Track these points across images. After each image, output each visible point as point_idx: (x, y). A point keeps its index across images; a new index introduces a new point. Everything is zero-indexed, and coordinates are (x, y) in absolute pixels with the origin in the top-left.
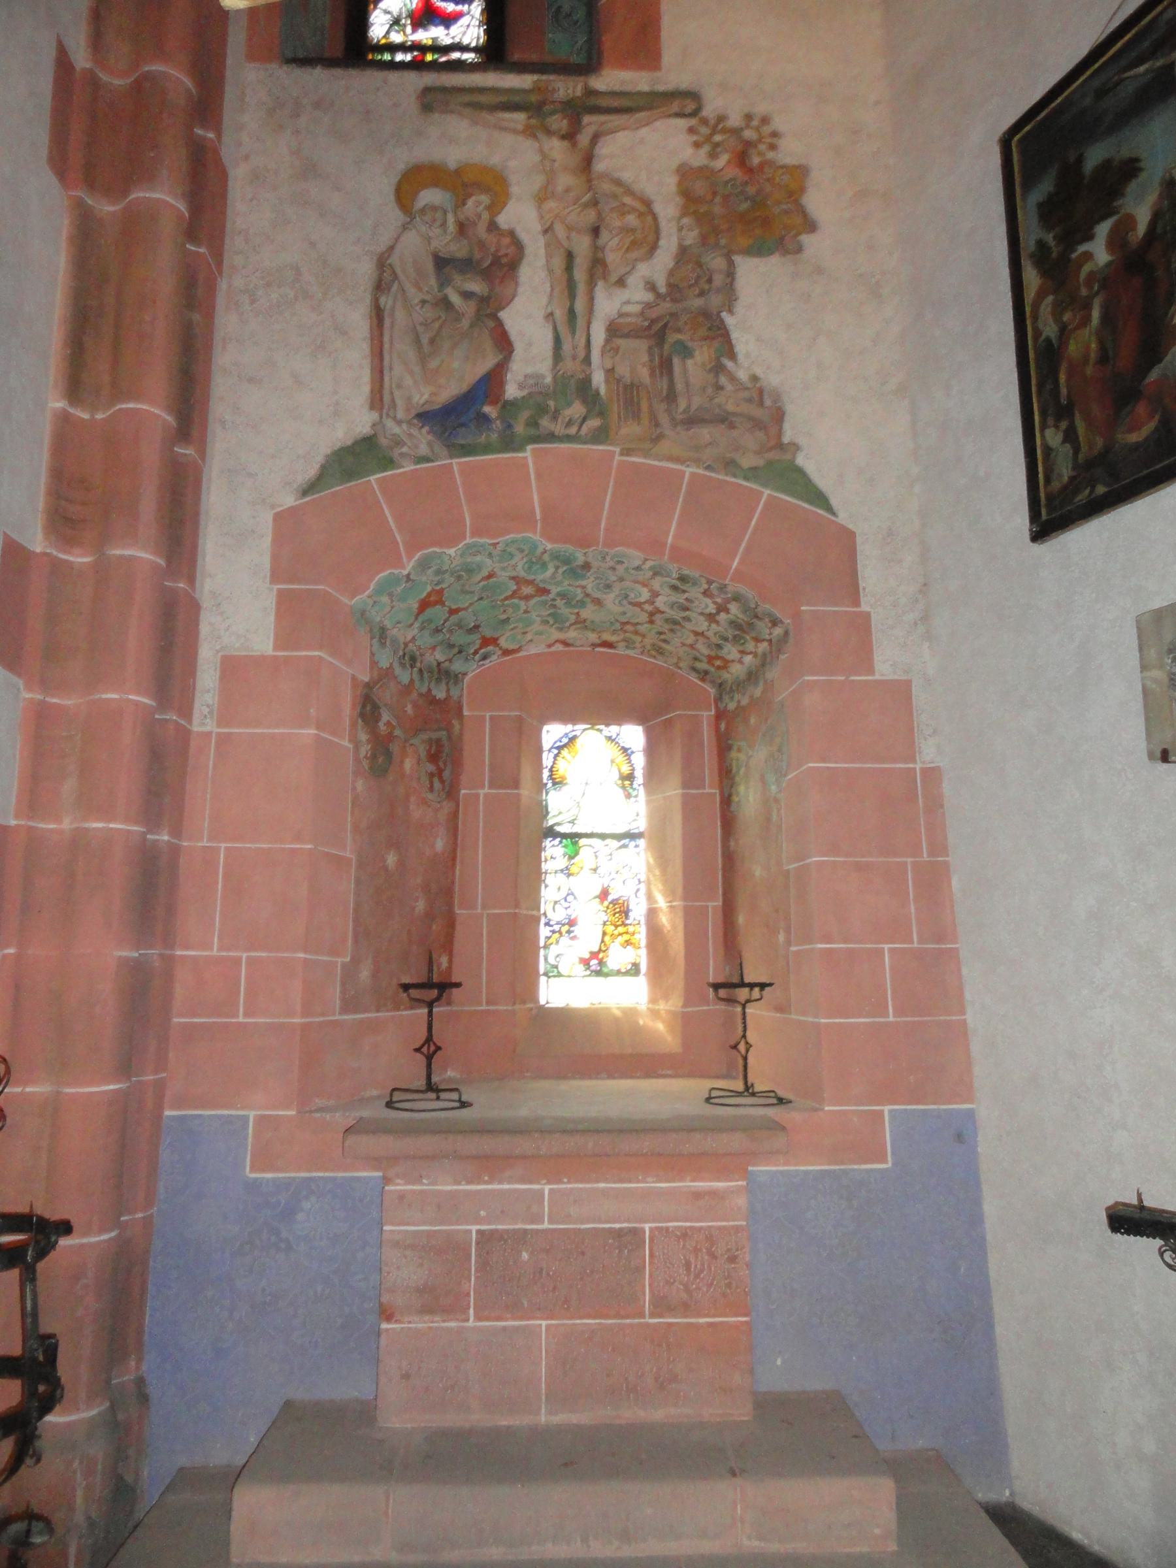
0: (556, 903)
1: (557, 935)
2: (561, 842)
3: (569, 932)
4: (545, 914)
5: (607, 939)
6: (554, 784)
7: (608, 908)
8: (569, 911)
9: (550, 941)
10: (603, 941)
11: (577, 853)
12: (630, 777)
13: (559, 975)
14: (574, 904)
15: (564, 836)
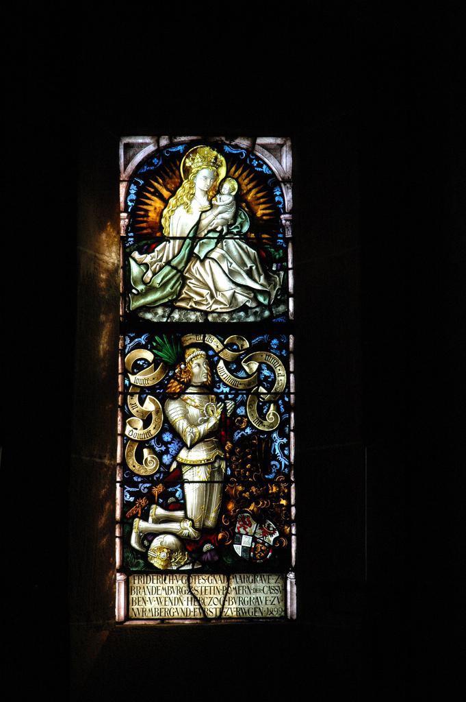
0: (142, 444)
1: (143, 501)
2: (149, 340)
3: (165, 495)
4: (124, 464)
5: (231, 506)
6: (138, 239)
7: (232, 452)
8: (166, 459)
9: (133, 510)
10: (223, 510)
11: (181, 358)
12: (272, 224)
13: (150, 570)
14: (173, 448)
15: (154, 329)
